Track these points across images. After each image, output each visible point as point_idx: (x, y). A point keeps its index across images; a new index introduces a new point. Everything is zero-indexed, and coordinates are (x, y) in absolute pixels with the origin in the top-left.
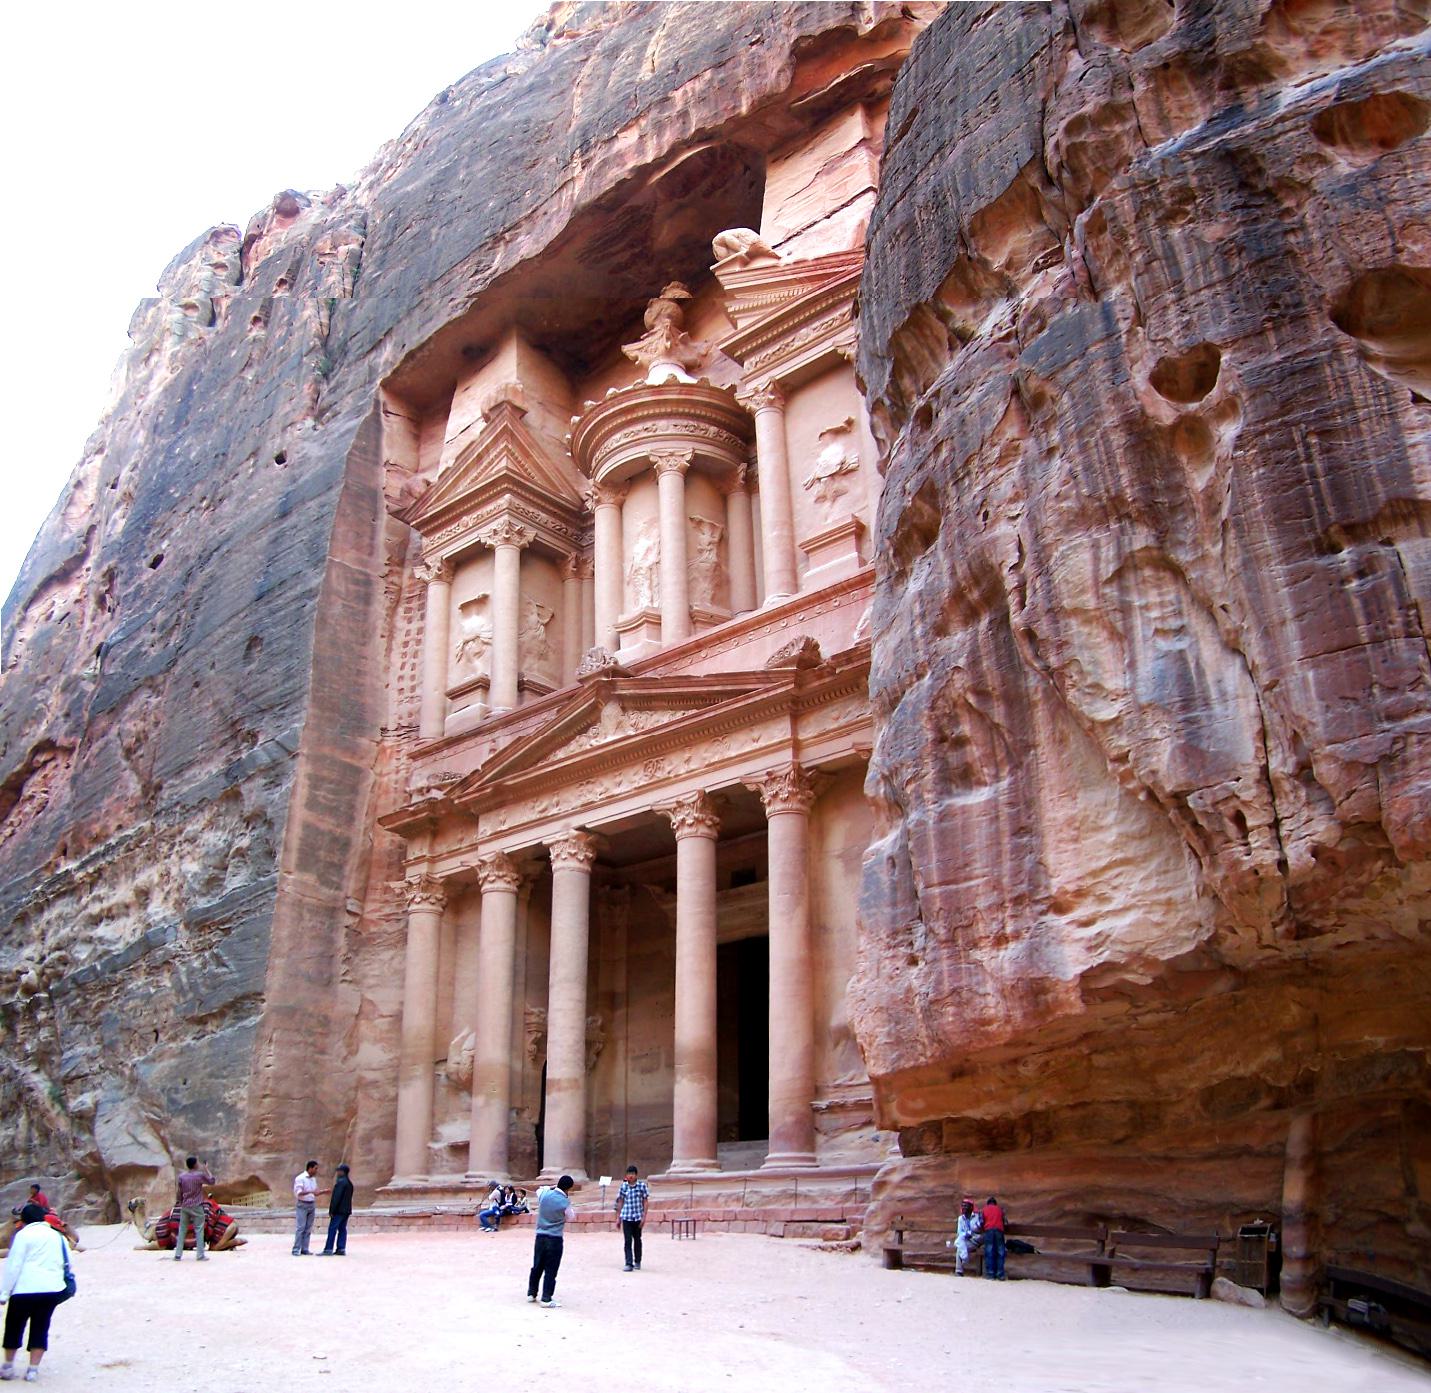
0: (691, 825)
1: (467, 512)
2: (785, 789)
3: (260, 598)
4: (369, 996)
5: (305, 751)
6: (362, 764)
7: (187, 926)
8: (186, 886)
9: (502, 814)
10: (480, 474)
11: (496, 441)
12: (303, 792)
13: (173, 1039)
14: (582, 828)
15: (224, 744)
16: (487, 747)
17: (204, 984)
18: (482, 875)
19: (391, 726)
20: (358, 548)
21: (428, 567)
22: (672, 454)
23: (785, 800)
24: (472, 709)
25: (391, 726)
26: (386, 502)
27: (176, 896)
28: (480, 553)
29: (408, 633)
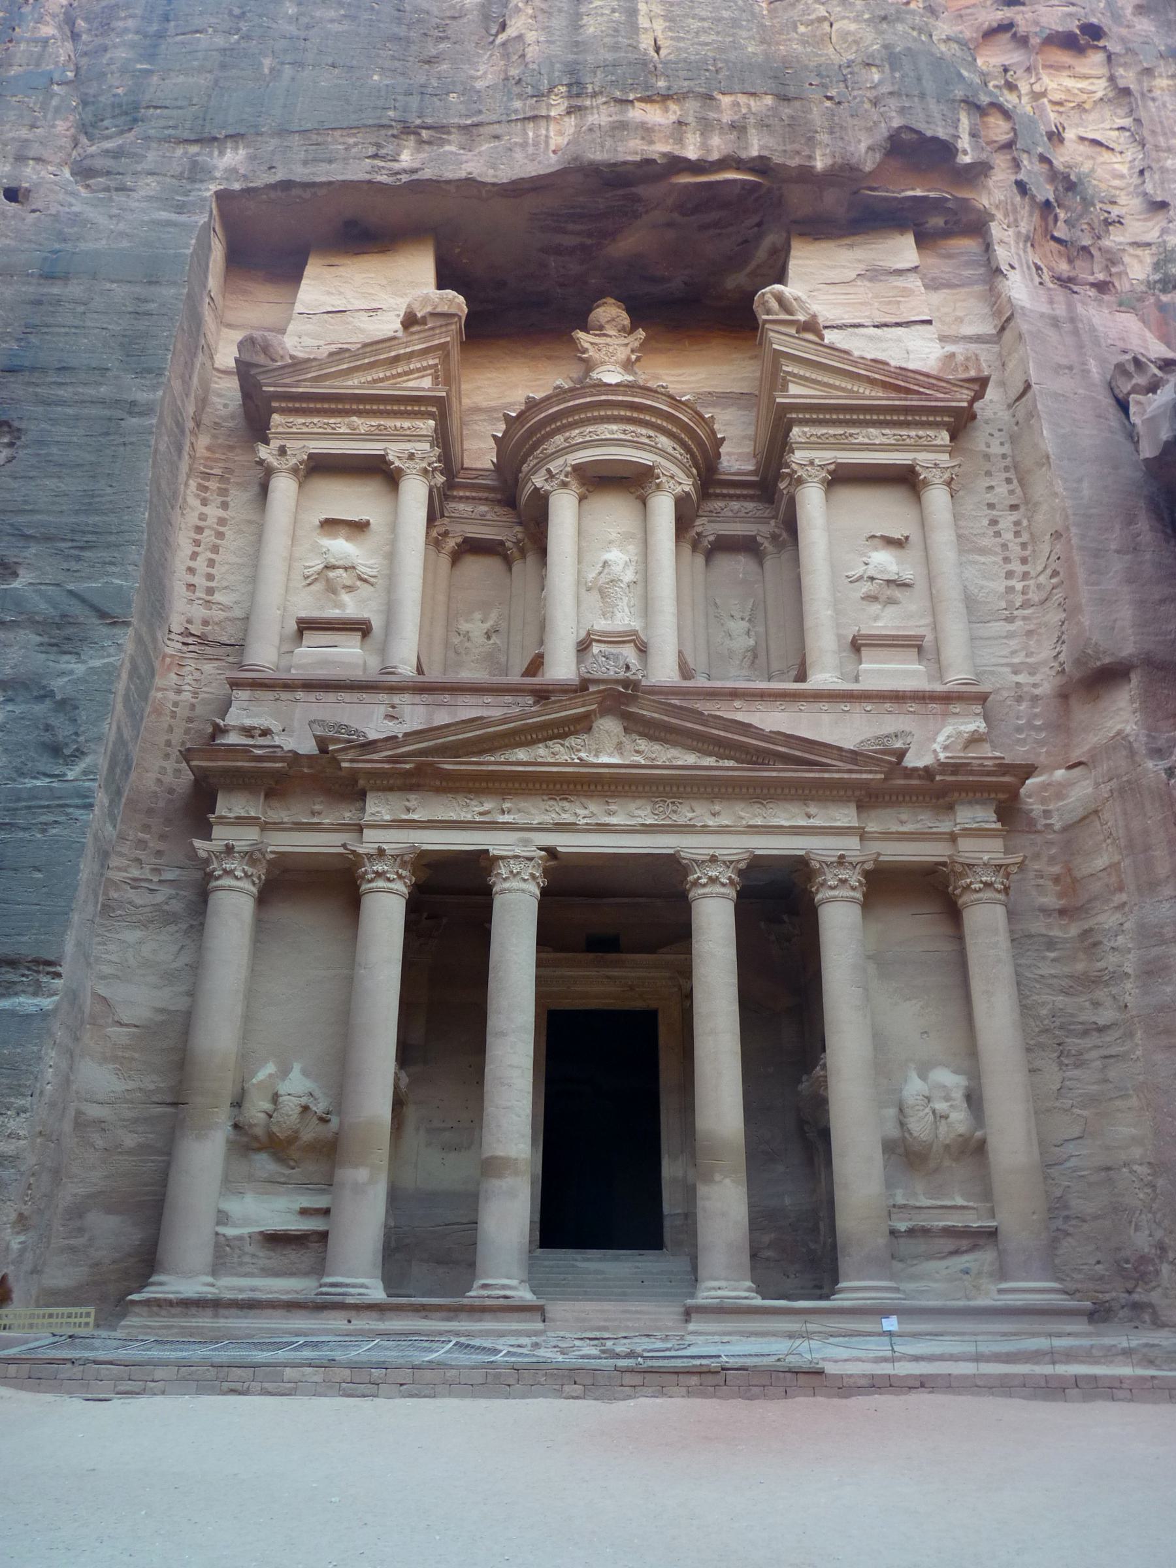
0: (724, 885)
1: (359, 413)
2: (855, 878)
6: (157, 664)
9: (413, 799)
10: (387, 378)
12: (124, 675)
14: (551, 852)
16: (382, 710)
18: (379, 868)
19: (177, 627)
20: (184, 382)
21: (282, 451)
22: (672, 477)
23: (853, 888)
24: (348, 655)
25: (177, 627)
26: (203, 342)
28: (381, 472)
29: (203, 517)
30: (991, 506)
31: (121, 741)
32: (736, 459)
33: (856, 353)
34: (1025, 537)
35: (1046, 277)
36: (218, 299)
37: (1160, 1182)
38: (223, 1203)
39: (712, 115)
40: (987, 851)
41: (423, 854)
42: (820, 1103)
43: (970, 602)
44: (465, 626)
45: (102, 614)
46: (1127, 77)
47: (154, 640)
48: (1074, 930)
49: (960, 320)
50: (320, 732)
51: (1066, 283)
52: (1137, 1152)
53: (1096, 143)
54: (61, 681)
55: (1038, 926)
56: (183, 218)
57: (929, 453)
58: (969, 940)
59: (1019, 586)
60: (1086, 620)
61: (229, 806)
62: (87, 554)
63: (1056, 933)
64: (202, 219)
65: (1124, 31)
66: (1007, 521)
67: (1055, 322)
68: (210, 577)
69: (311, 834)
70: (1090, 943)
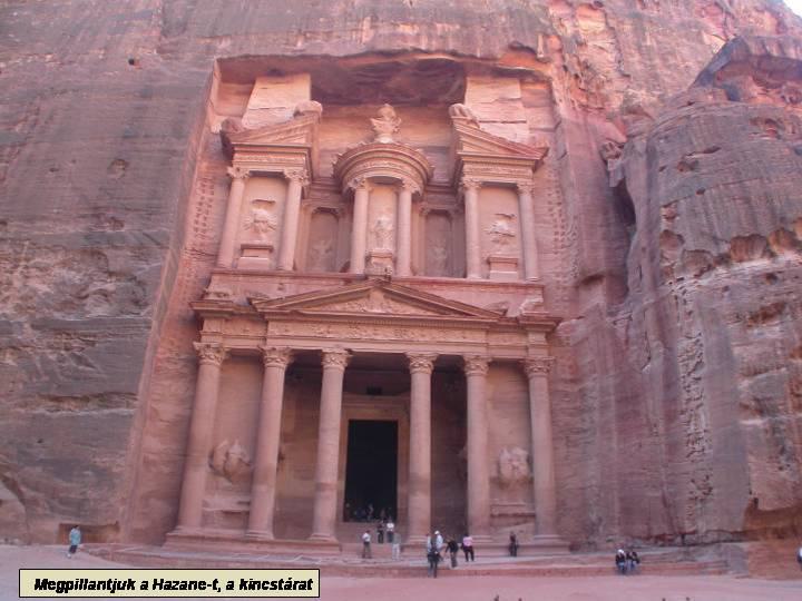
2: (483, 365)
3: (125, 137)
4: (154, 406)
5: (171, 247)
7: (33, 326)
8: (36, 299)
9: (290, 326)
11: (304, 127)
13: (25, 405)
14: (350, 351)
15: (83, 217)
16: (277, 286)
17: (62, 374)
18: (273, 356)
21: (238, 170)
24: (263, 261)
27: (19, 302)
29: (203, 198)
30: (550, 203)
31: (164, 298)
32: (440, 177)
33: (493, 134)
34: (563, 217)
35: (576, 105)
36: (215, 104)
37: (602, 495)
38: (205, 496)
39: (432, 31)
40: (541, 355)
41: (293, 350)
42: (465, 462)
43: (539, 245)
44: (316, 247)
45: (158, 244)
46: (612, 23)
47: (179, 253)
48: (576, 388)
49: (539, 121)
50: (248, 295)
51: (585, 108)
52: (594, 482)
53: (601, 48)
54: (140, 273)
55: (561, 387)
56: (202, 71)
57: (523, 178)
58: (531, 393)
59: (560, 238)
60: (585, 255)
61: (210, 326)
62: (153, 217)
63: (569, 389)
64: (209, 71)
65: (612, 5)
66: (556, 209)
67: (578, 125)
68: (205, 225)
69: (244, 338)
70: (582, 394)
